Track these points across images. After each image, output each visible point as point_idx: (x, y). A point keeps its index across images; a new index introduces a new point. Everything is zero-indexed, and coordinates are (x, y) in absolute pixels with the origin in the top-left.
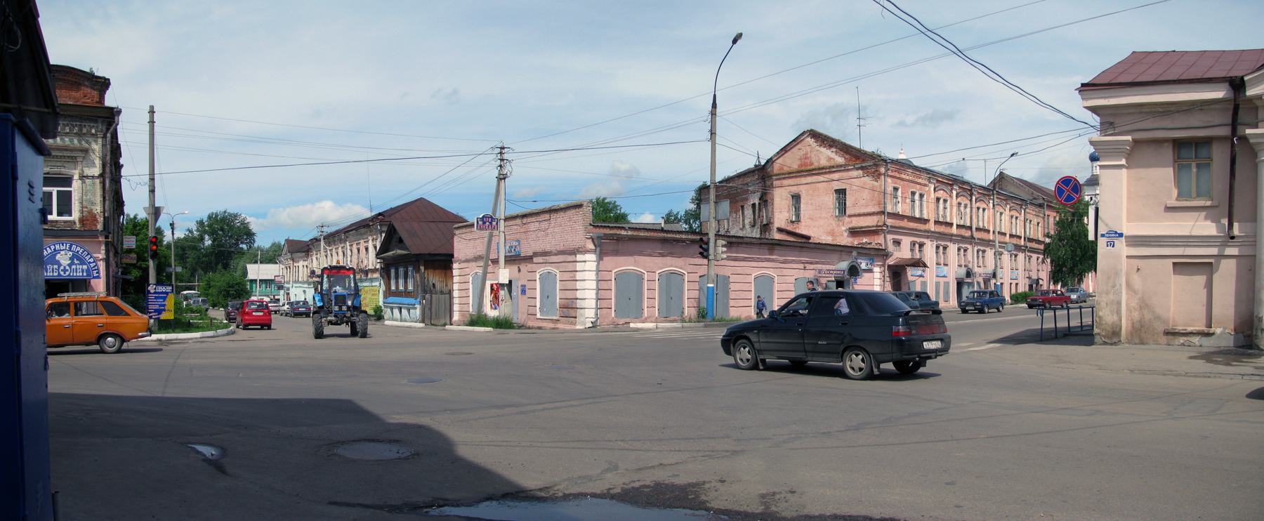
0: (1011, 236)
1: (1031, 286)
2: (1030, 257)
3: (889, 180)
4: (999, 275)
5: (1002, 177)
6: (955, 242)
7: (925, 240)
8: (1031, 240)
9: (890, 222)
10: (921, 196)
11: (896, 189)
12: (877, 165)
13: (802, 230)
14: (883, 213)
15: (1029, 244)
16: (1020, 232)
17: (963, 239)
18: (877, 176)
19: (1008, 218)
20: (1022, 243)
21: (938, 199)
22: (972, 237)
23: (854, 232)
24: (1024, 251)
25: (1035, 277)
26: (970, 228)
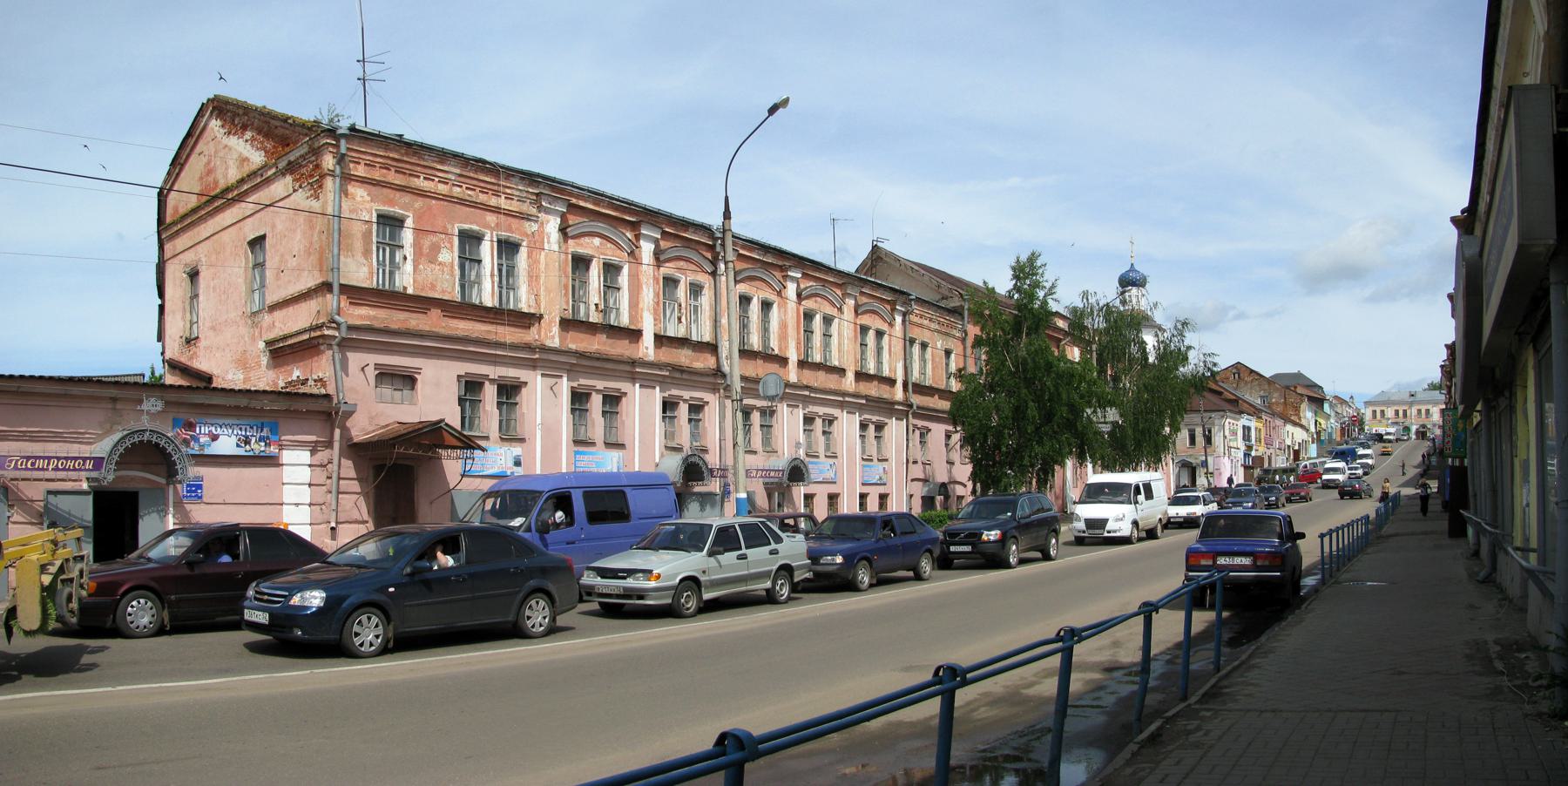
0: (861, 376)
1: (928, 501)
2: (924, 432)
3: (359, 193)
4: (819, 469)
5: (877, 257)
6: (648, 382)
7: (624, 386)
8: (920, 389)
9: (362, 314)
10: (507, 248)
11: (390, 223)
12: (316, 152)
13: (202, 364)
14: (326, 287)
15: (917, 400)
16: (892, 366)
17: (681, 375)
18: (312, 179)
19: (898, 346)
20: (899, 394)
21: (809, 316)
22: (718, 372)
23: (281, 352)
24: (902, 415)
25: (942, 477)
26: (712, 348)
